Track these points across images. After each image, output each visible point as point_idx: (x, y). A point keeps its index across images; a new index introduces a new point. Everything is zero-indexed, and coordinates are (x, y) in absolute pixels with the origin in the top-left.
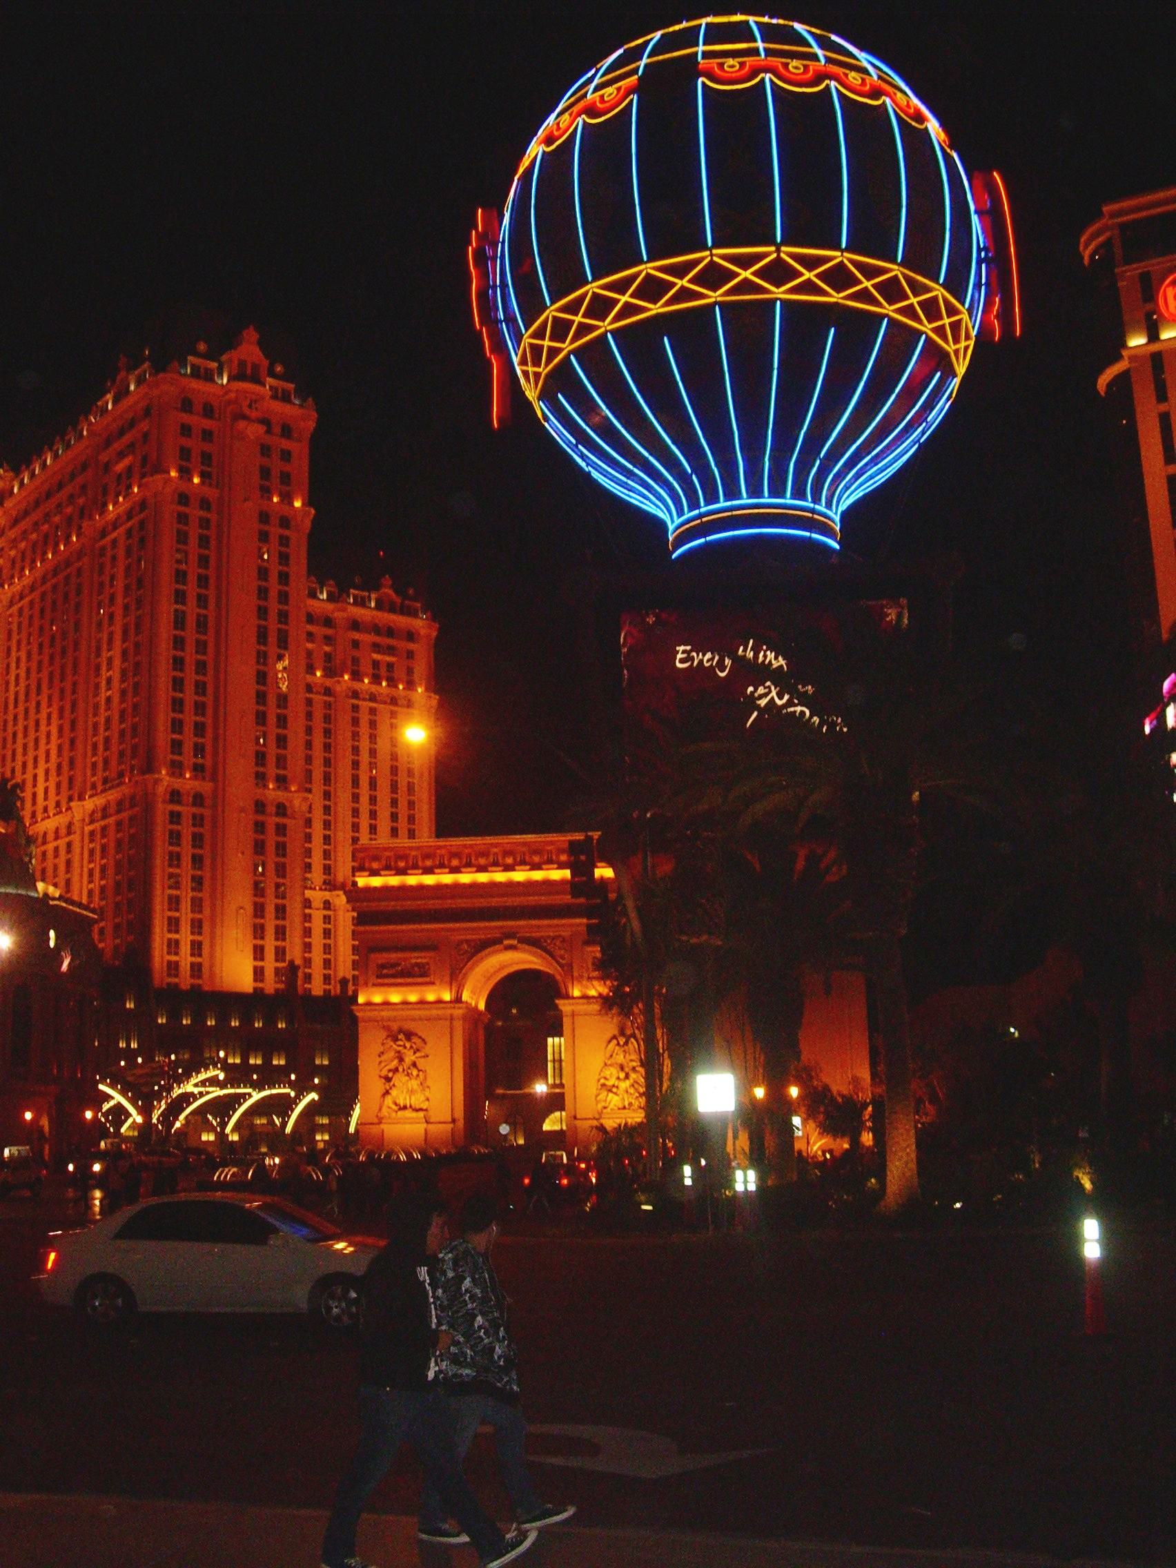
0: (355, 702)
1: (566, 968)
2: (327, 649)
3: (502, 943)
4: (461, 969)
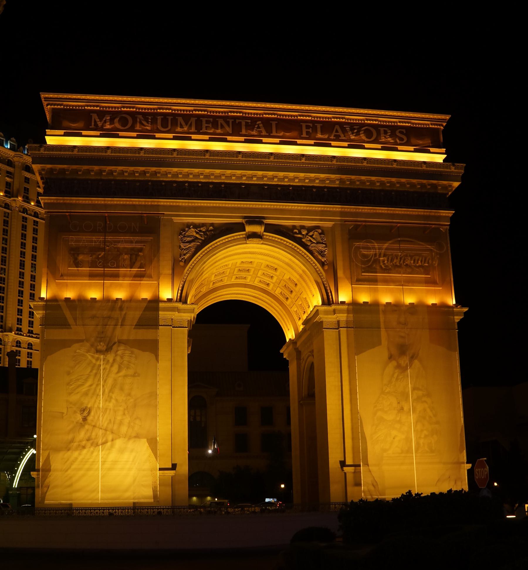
0: (25, 215)
1: (326, 267)
2: (8, 179)
3: (244, 230)
4: (187, 262)
